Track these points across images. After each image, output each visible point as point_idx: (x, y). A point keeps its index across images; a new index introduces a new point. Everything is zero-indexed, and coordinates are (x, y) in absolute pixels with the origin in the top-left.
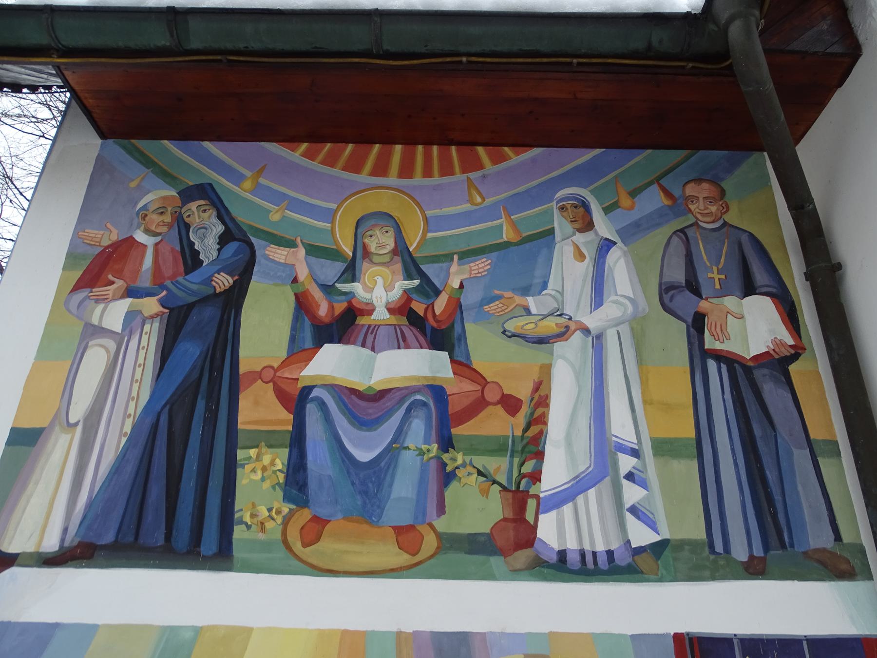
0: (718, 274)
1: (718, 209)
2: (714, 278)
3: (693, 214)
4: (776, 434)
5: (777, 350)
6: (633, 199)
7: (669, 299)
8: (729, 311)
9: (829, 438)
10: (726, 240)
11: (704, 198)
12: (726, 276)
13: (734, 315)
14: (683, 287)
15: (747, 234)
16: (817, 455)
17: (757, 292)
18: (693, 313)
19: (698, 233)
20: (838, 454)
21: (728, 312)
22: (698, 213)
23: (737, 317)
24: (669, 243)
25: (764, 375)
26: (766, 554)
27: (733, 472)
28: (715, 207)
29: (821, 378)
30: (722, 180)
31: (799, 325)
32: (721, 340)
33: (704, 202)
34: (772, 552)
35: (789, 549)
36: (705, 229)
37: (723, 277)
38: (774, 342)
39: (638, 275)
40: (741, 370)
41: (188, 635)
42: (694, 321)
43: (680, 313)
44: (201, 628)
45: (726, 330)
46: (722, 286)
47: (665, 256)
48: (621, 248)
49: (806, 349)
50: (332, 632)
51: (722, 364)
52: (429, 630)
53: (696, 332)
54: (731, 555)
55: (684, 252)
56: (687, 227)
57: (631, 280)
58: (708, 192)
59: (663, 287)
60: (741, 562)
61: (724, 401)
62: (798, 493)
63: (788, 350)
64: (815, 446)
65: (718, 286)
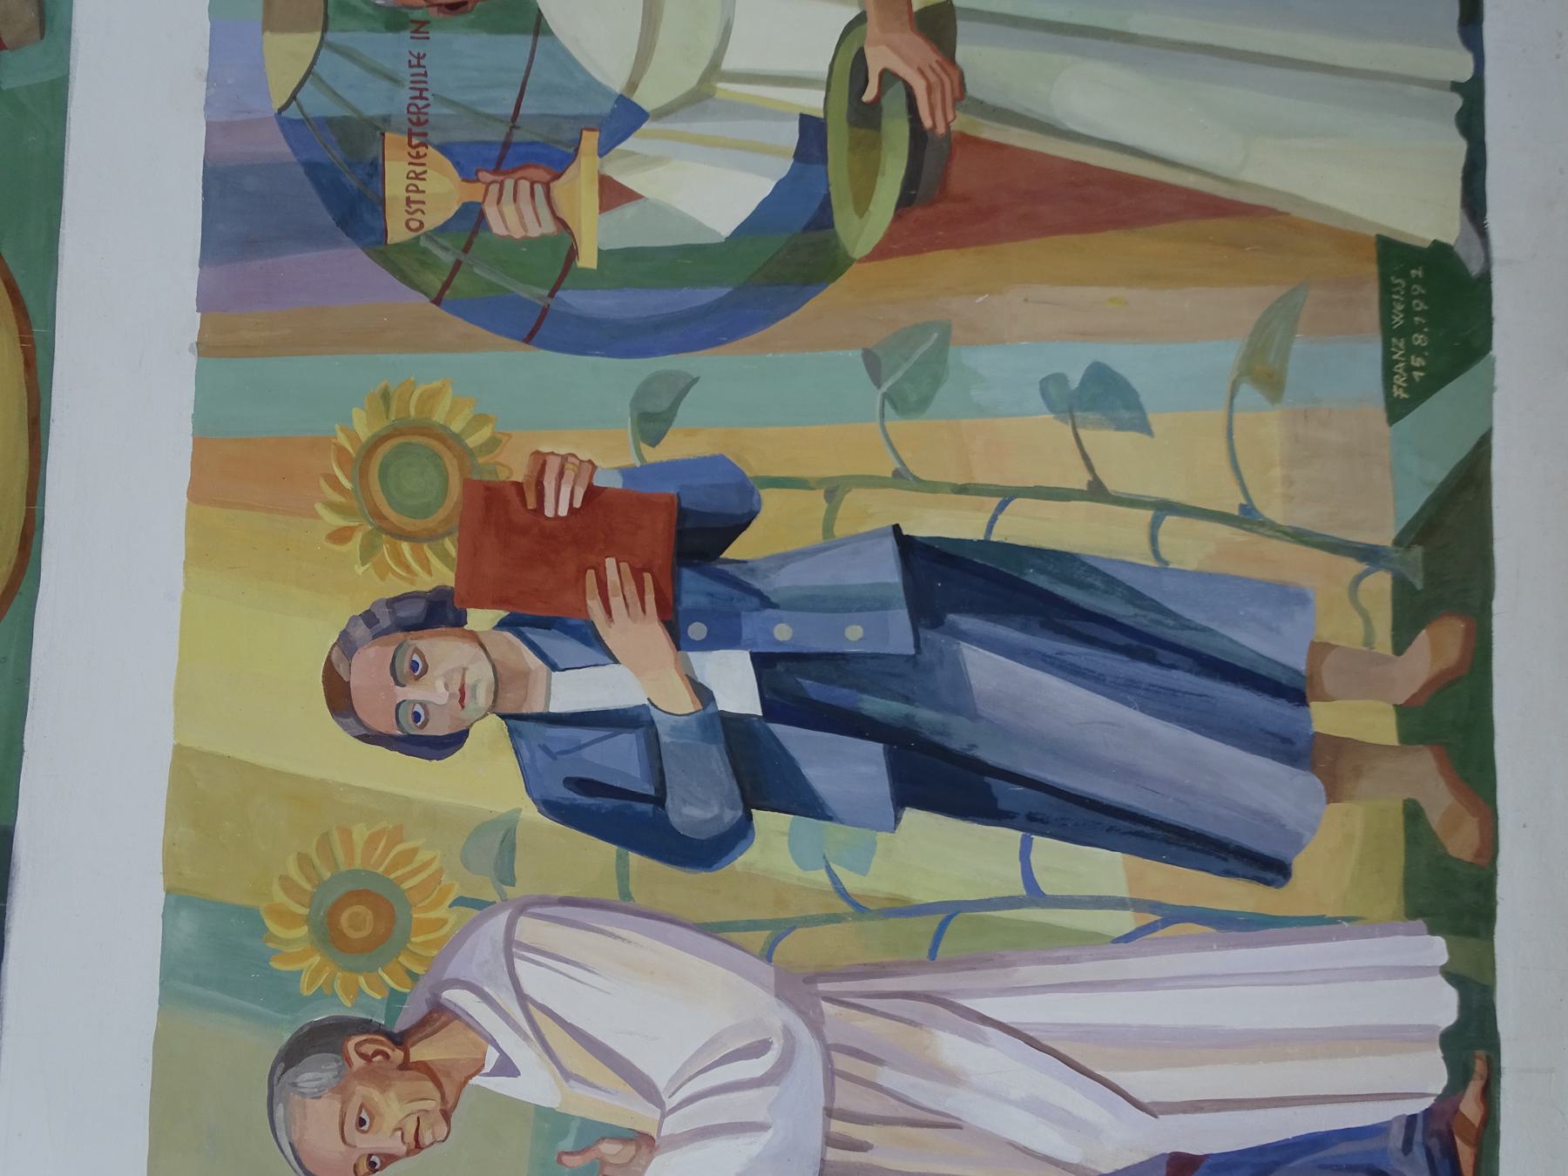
41: (187, 923)
44: (168, 892)
50: (196, 532)
52: (198, 269)
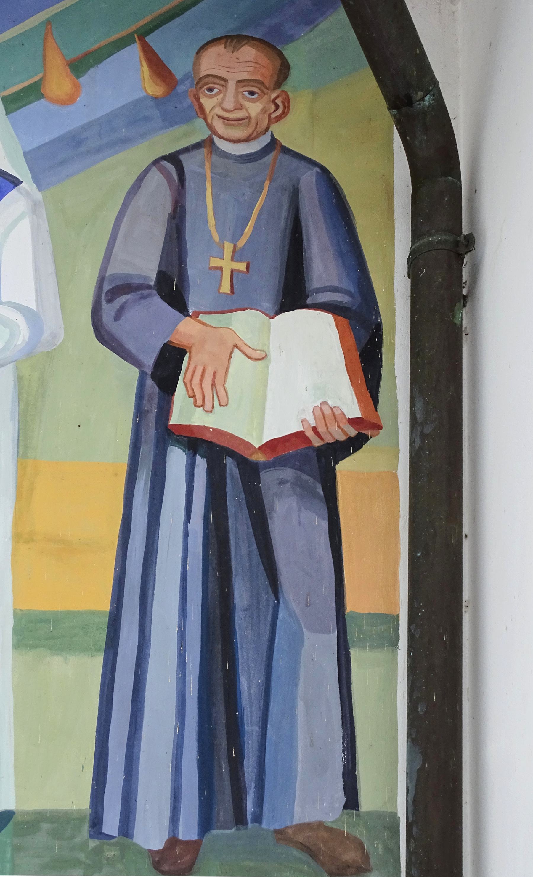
0: (232, 260)
1: (264, 110)
2: (221, 269)
3: (205, 119)
4: (279, 603)
5: (321, 430)
6: (78, 77)
7: (113, 314)
8: (239, 343)
9: (383, 610)
10: (267, 183)
11: (239, 81)
12: (248, 268)
13: (249, 351)
14: (149, 287)
15: (317, 169)
16: (350, 642)
17: (309, 301)
18: (159, 346)
19: (207, 165)
20: (394, 643)
21: (236, 346)
22: (219, 117)
23: (254, 357)
24: (139, 187)
25: (282, 482)
26: (203, 836)
27: (172, 679)
28: (258, 104)
29: (398, 487)
30: (291, 39)
31: (380, 375)
32: (208, 406)
33: (237, 89)
34: (215, 832)
35: (250, 825)
36: (225, 155)
37: (242, 266)
38: (318, 413)
39: (55, 256)
40: (236, 472)
42: (158, 364)
43: (131, 346)
45: (224, 384)
46: (236, 286)
47: (124, 215)
48: (28, 194)
49: (380, 428)
51: (198, 457)
53: (157, 388)
54: (132, 838)
55: (169, 208)
56: (186, 150)
57: (36, 269)
58: (251, 69)
59: (106, 287)
60: (150, 851)
61: (186, 534)
62: (293, 716)
63: (346, 429)
64: (351, 627)
65: (226, 288)
